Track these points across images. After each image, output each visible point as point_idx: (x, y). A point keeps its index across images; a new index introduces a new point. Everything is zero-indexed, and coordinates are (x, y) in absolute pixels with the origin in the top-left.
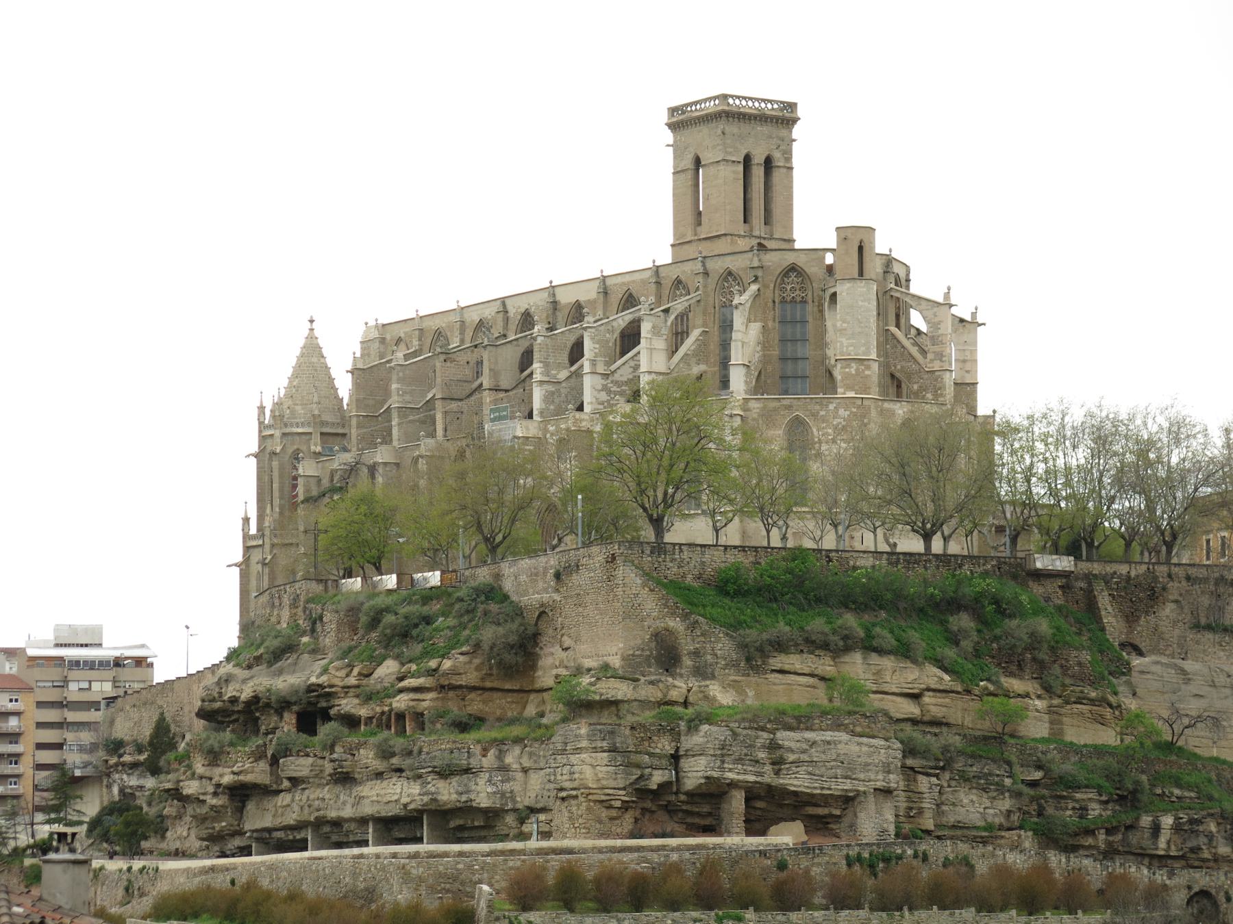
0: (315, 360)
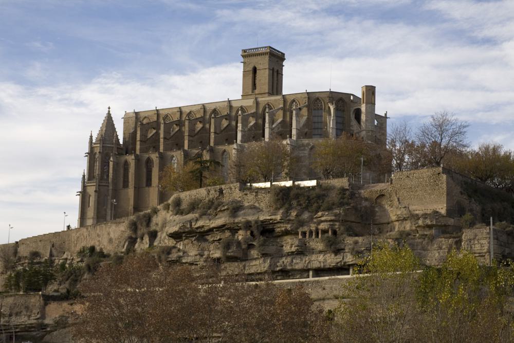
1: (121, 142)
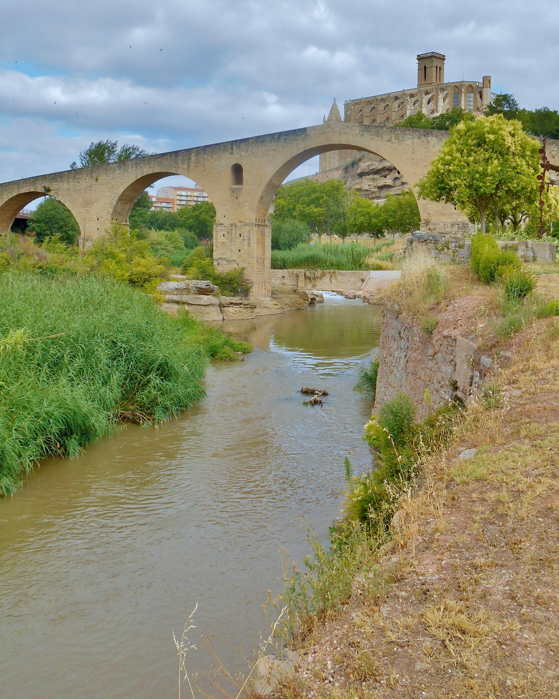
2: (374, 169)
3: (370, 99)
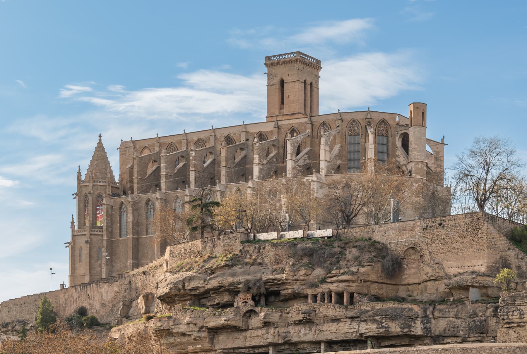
0: (103, 154)
1: (117, 180)
2: (197, 288)
3: (174, 140)
